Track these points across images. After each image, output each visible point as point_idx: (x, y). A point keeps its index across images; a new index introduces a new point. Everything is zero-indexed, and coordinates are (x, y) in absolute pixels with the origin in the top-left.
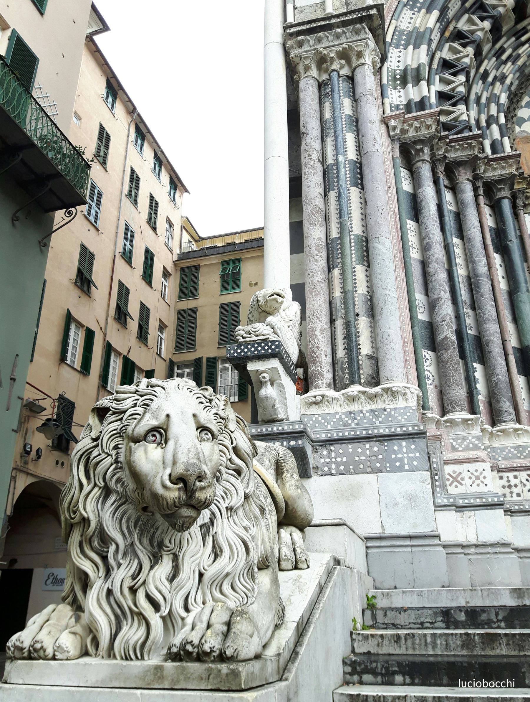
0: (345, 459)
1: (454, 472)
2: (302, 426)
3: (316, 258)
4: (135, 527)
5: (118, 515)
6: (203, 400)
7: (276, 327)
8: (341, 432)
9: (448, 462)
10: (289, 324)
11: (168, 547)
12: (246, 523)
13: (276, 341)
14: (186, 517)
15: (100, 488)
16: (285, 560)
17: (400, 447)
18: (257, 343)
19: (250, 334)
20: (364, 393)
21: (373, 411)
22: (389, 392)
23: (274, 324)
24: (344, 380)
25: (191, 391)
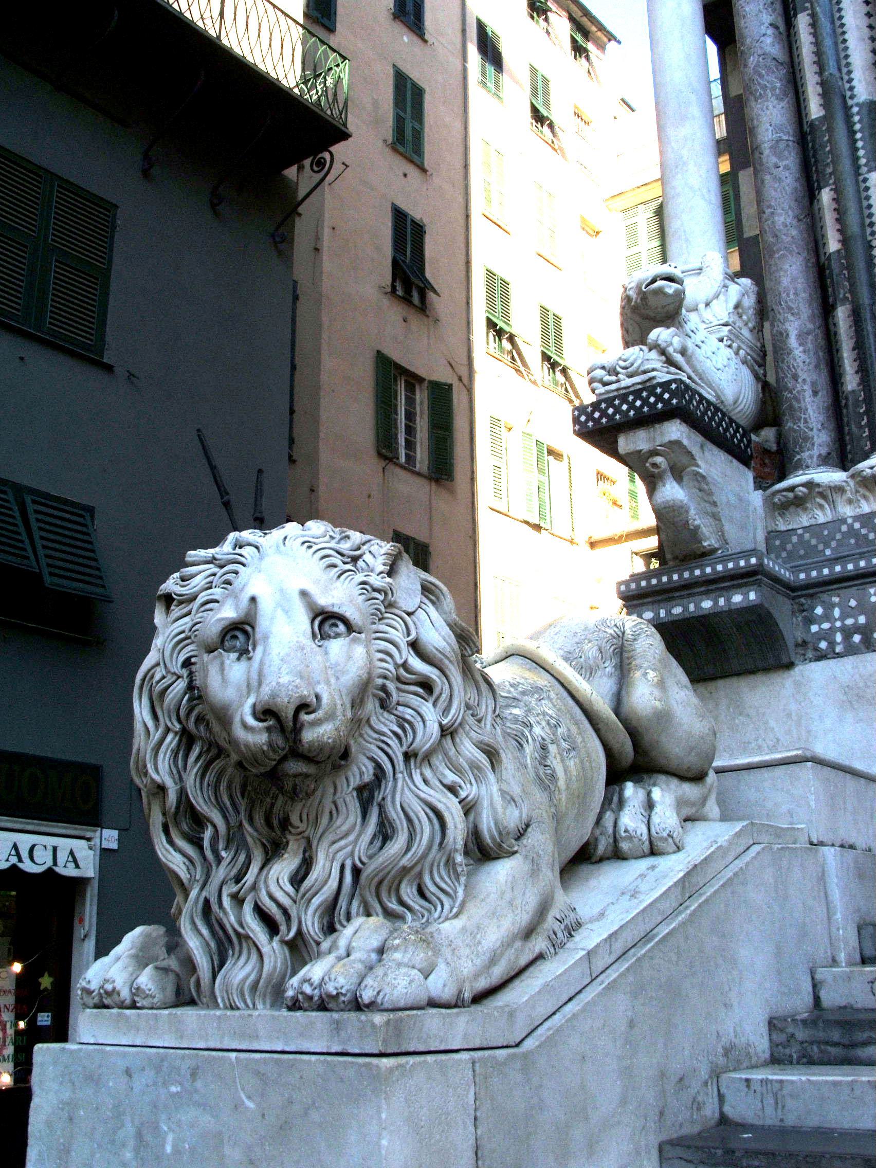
2: (753, 561)
3: (775, 171)
4: (243, 798)
5: (210, 777)
6: (337, 560)
7: (670, 350)
10: (719, 335)
11: (298, 827)
13: (669, 383)
14: (296, 776)
15: (176, 733)
16: (625, 839)
18: (632, 393)
19: (617, 374)
23: (663, 345)
24: (862, 443)
25: (310, 547)
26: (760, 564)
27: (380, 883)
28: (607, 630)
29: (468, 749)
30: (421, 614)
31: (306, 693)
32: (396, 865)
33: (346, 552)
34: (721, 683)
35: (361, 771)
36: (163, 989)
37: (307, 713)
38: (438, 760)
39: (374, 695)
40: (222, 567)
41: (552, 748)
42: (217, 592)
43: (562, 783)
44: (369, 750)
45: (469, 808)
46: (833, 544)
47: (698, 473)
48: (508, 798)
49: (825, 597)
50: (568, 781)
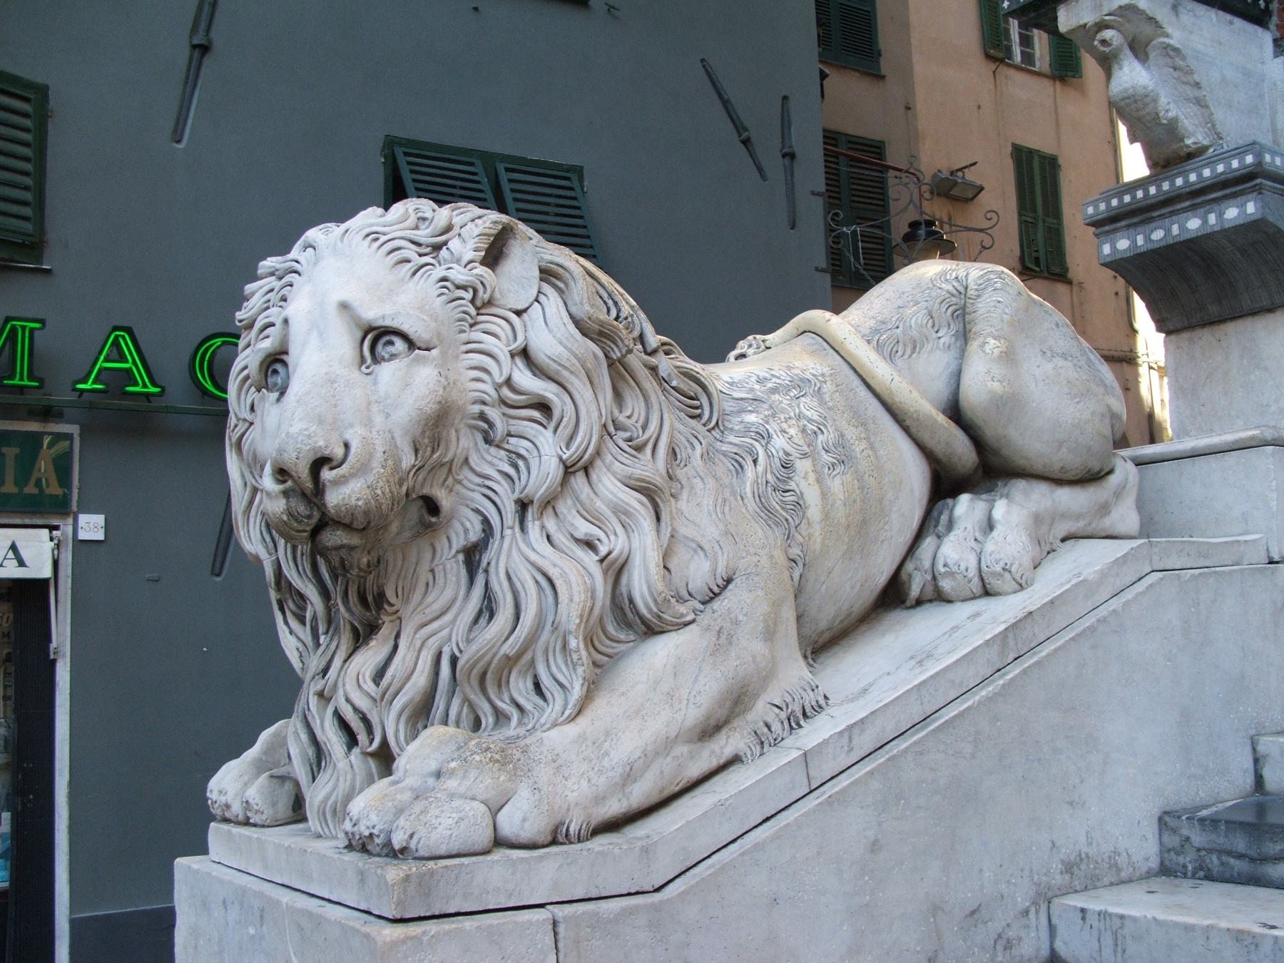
2: (1249, 159)
6: (410, 252)
11: (392, 605)
25: (377, 239)
26: (1259, 163)
28: (943, 286)
31: (321, 443)
32: (495, 655)
33: (422, 240)
34: (1230, 327)
35: (465, 529)
36: (274, 804)
37: (332, 469)
38: (565, 506)
41: (803, 466)
43: (814, 512)
44: (472, 500)
47: (1169, 45)
48: (694, 546)
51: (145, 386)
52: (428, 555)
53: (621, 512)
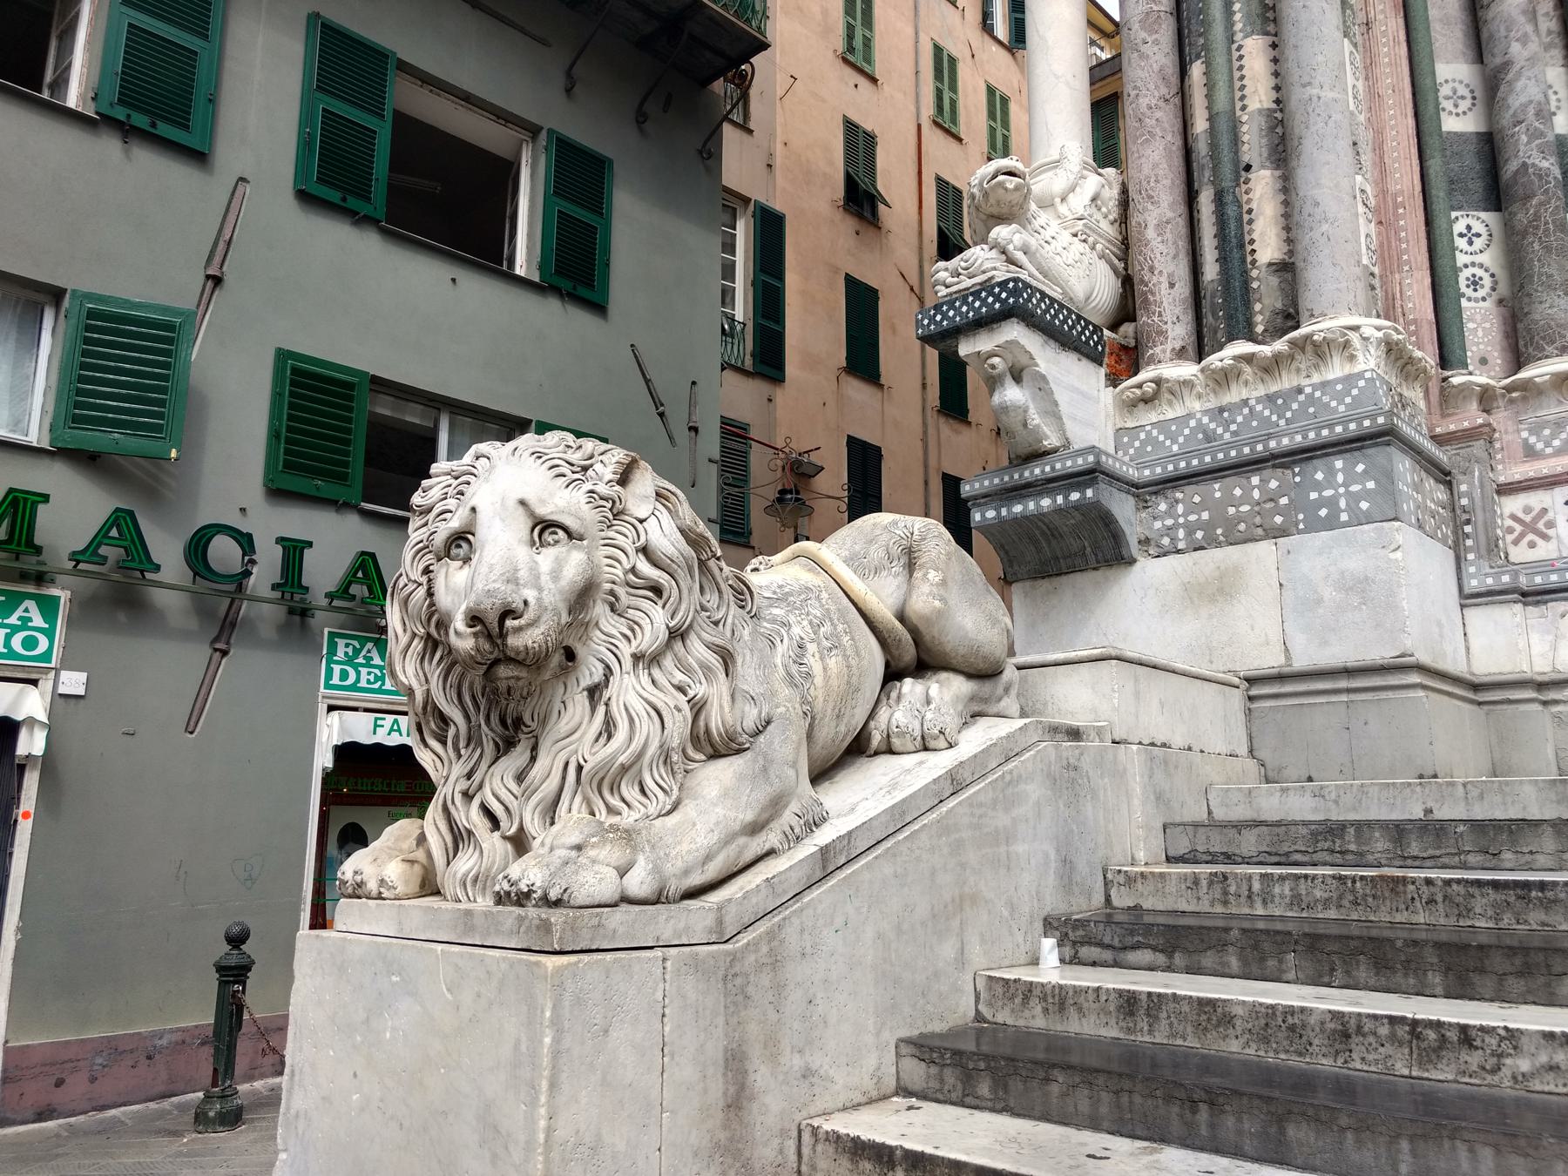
0: (1205, 516)
1: (1527, 510)
2: (1091, 458)
3: (1144, 48)
6: (566, 469)
7: (1011, 247)
8: (1194, 457)
9: (1506, 490)
10: (1074, 231)
12: (680, 677)
13: (1006, 282)
16: (899, 735)
17: (1331, 473)
20: (1249, 359)
21: (1270, 399)
22: (1309, 348)
23: (1003, 243)
27: (603, 779)
29: (697, 650)
30: (652, 521)
34: (1064, 579)
35: (591, 672)
36: (406, 882)
38: (668, 662)
39: (605, 601)
40: (456, 478)
41: (812, 648)
42: (451, 503)
43: (819, 680)
45: (698, 707)
46: (1181, 440)
49: (1169, 493)
50: (827, 678)
51: (141, 562)
52: (561, 690)
53: (707, 669)
